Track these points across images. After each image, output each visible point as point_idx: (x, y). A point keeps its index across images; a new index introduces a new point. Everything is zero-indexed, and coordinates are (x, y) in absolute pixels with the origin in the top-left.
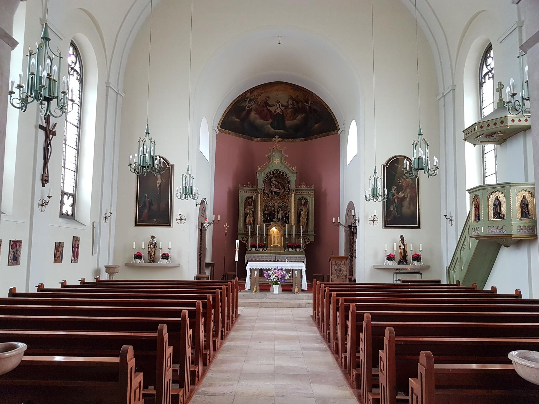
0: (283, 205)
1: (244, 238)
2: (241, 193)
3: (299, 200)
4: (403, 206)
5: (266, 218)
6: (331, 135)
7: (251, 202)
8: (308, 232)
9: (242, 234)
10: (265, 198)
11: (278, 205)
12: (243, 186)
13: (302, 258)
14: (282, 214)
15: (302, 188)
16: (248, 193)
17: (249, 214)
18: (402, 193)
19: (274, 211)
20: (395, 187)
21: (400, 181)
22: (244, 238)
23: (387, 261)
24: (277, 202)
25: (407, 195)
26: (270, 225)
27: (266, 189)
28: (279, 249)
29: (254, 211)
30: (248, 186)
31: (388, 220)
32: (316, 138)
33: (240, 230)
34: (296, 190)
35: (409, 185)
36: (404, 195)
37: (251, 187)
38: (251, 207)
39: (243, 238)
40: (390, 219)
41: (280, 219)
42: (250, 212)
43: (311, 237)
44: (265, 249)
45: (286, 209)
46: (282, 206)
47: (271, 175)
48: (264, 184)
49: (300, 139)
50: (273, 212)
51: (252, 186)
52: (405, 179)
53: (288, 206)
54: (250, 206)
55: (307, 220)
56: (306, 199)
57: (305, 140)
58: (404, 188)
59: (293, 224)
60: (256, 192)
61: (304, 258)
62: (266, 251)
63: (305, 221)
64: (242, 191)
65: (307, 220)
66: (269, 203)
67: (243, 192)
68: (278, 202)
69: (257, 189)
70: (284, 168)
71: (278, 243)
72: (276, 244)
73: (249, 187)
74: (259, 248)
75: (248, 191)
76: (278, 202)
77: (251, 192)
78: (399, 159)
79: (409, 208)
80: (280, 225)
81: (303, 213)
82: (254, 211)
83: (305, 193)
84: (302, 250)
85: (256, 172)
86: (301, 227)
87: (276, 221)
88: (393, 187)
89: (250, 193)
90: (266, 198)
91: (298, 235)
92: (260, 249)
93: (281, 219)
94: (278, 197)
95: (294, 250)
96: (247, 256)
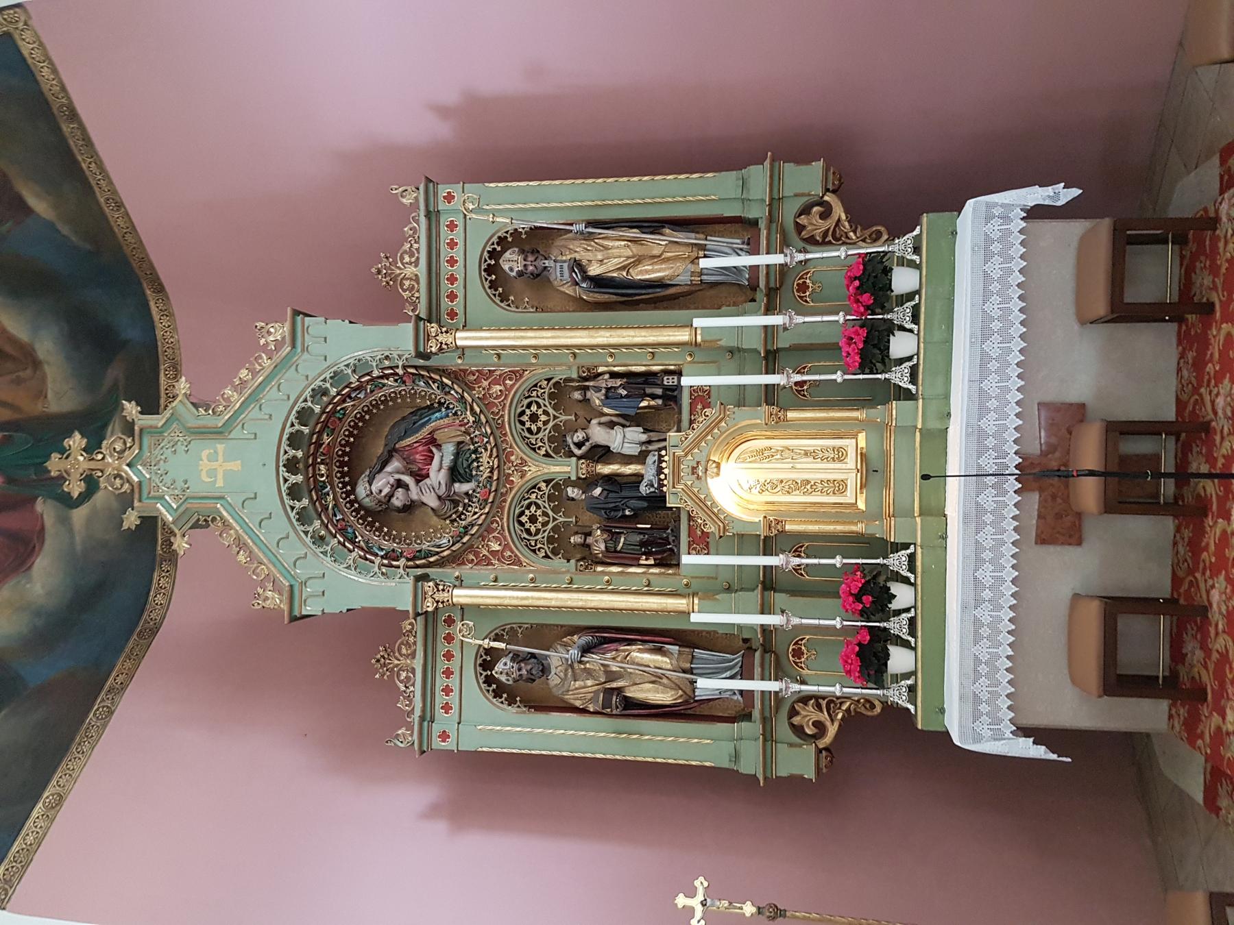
0: (549, 417)
1: (796, 720)
2: (453, 735)
3: (504, 298)
5: (642, 544)
6: (63, 89)
7: (516, 657)
8: (752, 214)
9: (768, 737)
10: (493, 553)
11: (547, 455)
12: (402, 719)
13: (995, 227)
14: (611, 425)
15: (417, 280)
16: (454, 682)
17: (611, 676)
19: (586, 483)
22: (796, 720)
24: (523, 463)
26: (690, 518)
27: (425, 546)
28: (891, 444)
29: (585, 639)
30: (404, 675)
32: (120, 205)
33: (736, 756)
34: (433, 315)
37: (413, 655)
38: (556, 658)
39: (798, 730)
41: (649, 442)
42: (589, 673)
43: (788, 191)
44: (897, 561)
45: (577, 395)
46: (556, 427)
47: (326, 508)
48: (391, 556)
49: (156, 317)
50: (598, 491)
51: (404, 651)
53: (549, 380)
54: (545, 670)
55: (654, 226)
56: (501, 240)
57: (160, 289)
59: (683, 336)
60: (450, 621)
61: (989, 206)
62: (912, 558)
63: (657, 243)
64: (437, 728)
65: (654, 226)
66: (533, 519)
67: (443, 721)
68: (519, 452)
69: (417, 615)
70: (266, 410)
71: (839, 455)
72: (849, 470)
73: (413, 671)
74: (887, 615)
75: (441, 682)
76: (519, 452)
77: (449, 656)
80: (692, 435)
81: (600, 257)
82: (585, 639)
83: (453, 253)
84: (900, 247)
85: (294, 619)
86: (704, 263)
87: (660, 470)
89: (455, 665)
90: (496, 547)
91: (771, 292)
92: (895, 605)
93: (646, 431)
94: (485, 458)
95: (901, 315)
96: (978, 739)
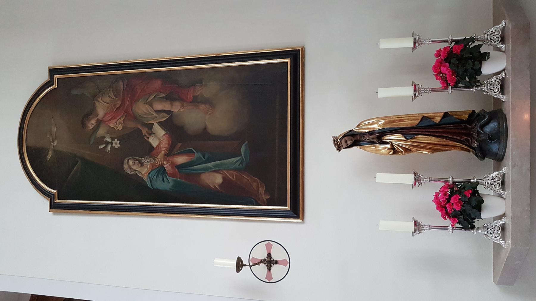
4: (205, 129)
18: (151, 133)
20: (131, 162)
21: (107, 143)
23: (477, 223)
25: (156, 111)
31: (265, 197)
35: (119, 103)
36: (161, 124)
40: (262, 190)
52: (99, 123)
58: (131, 125)
78: (32, 143)
79: (209, 102)
88: (129, 172)
